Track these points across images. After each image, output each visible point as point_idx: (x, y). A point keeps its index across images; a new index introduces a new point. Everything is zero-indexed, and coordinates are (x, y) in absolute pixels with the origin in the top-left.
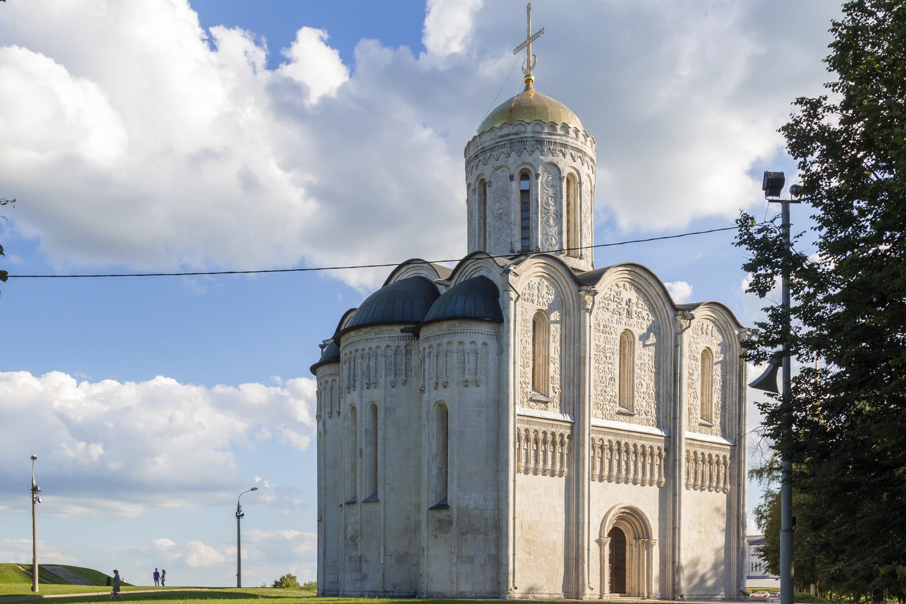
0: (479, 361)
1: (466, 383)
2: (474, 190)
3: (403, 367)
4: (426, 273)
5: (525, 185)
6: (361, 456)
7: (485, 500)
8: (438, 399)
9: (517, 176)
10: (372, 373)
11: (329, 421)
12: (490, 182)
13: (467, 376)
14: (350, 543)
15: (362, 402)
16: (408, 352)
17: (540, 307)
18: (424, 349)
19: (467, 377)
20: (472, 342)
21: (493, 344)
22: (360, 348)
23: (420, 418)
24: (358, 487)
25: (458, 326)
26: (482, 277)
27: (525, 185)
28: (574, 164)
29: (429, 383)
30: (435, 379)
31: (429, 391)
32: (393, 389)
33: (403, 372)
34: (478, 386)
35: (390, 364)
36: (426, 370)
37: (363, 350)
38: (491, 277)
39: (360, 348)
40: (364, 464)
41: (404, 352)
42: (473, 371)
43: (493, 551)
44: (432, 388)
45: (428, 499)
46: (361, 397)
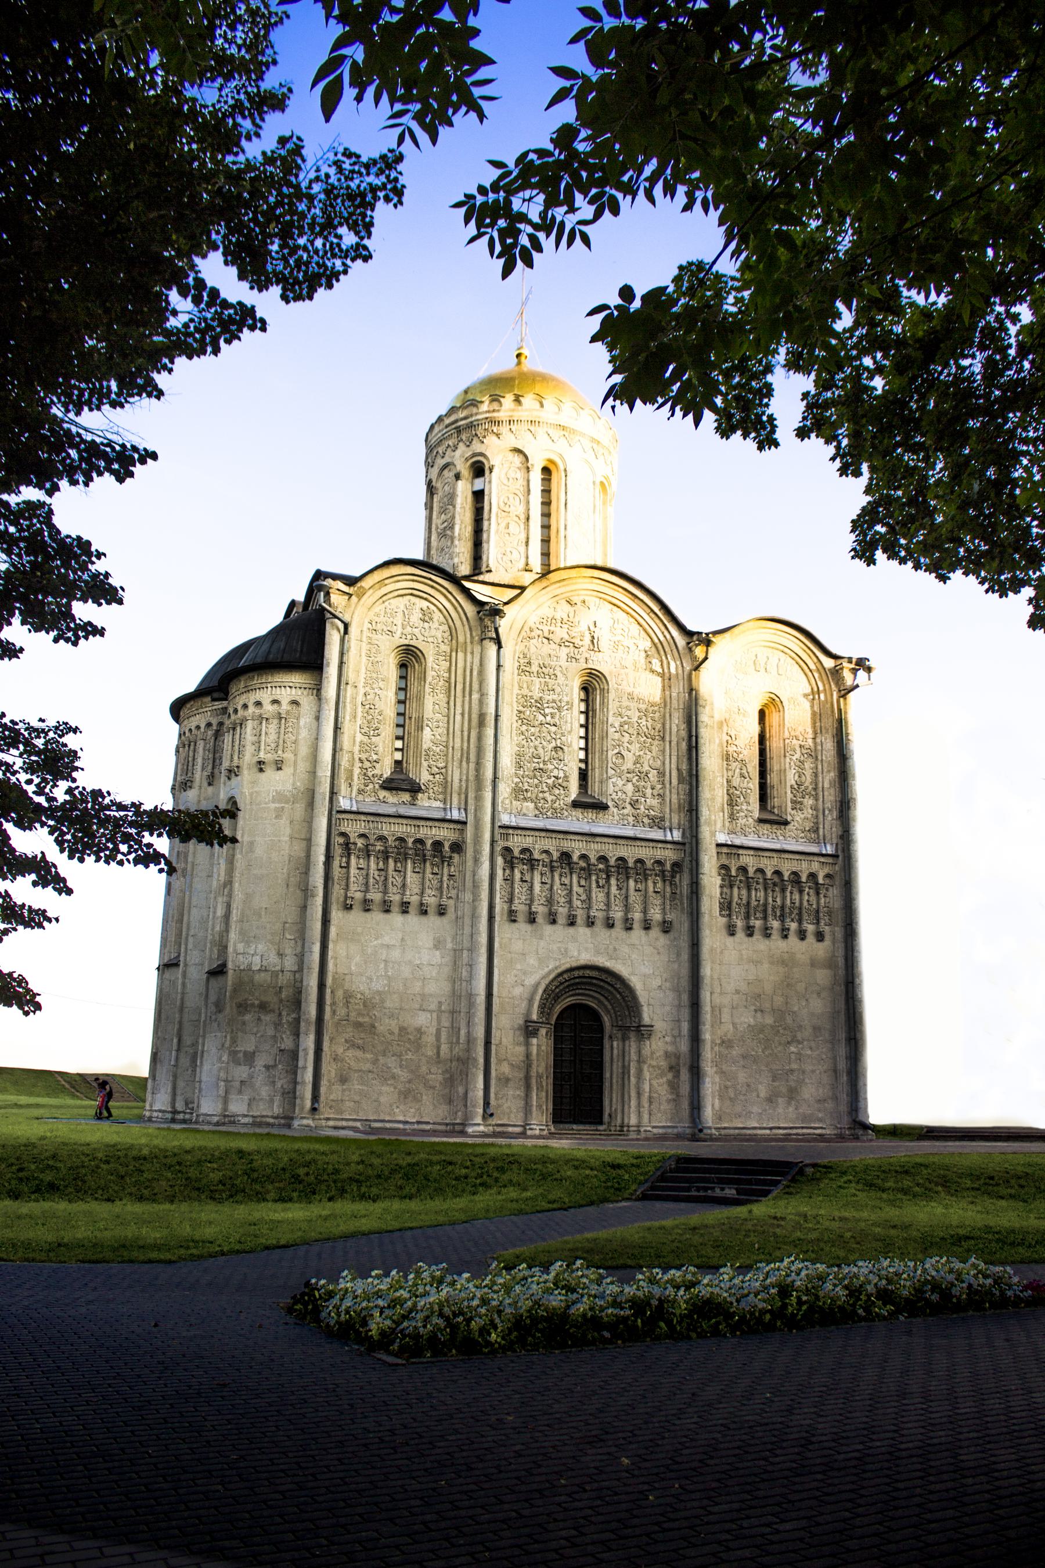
1: (261, 766)
5: (479, 484)
7: (281, 955)
9: (466, 473)
17: (406, 642)
20: (275, 702)
32: (210, 789)
42: (273, 745)
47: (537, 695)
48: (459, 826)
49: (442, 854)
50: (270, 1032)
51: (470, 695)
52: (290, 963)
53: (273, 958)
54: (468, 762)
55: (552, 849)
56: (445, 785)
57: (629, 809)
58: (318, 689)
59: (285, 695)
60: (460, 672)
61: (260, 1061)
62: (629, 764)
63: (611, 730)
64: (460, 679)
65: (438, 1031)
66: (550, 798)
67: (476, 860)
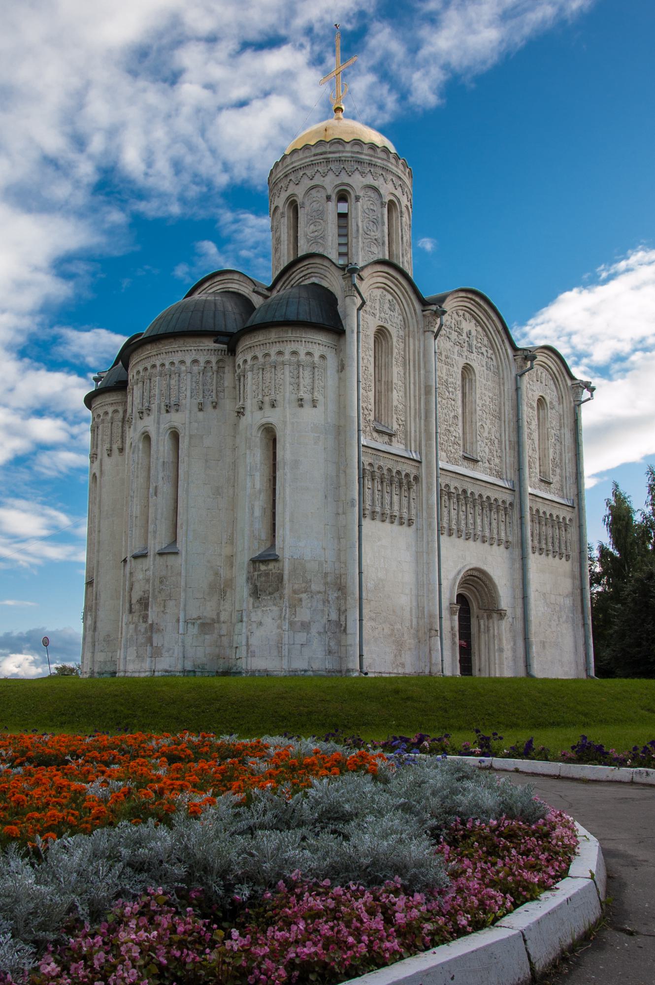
0: (316, 377)
1: (300, 402)
2: (283, 213)
3: (214, 387)
4: (236, 286)
5: (343, 208)
6: (156, 495)
8: (264, 421)
9: (334, 197)
10: (174, 393)
12: (303, 203)
13: (302, 393)
14: (136, 607)
15: (159, 428)
16: (220, 369)
17: (382, 324)
18: (245, 361)
19: (302, 394)
20: (309, 354)
21: (332, 362)
22: (158, 363)
23: (234, 448)
24: (150, 536)
25: (290, 334)
26: (314, 284)
27: (343, 208)
28: (396, 193)
29: (250, 404)
30: (260, 397)
31: (252, 412)
34: (315, 406)
35: (197, 383)
37: (163, 365)
38: (325, 284)
39: (158, 363)
40: (162, 503)
41: (215, 368)
42: (309, 388)
43: (334, 616)
45: (247, 548)
46: (158, 423)
47: (445, 378)
48: (417, 464)
49: (406, 483)
50: (320, 606)
51: (419, 371)
54: (420, 418)
55: (458, 486)
56: (406, 433)
57: (487, 465)
58: (339, 350)
59: (317, 351)
61: (314, 631)
62: (486, 434)
63: (478, 408)
64: (411, 358)
65: (411, 608)
66: (453, 451)
67: (429, 489)
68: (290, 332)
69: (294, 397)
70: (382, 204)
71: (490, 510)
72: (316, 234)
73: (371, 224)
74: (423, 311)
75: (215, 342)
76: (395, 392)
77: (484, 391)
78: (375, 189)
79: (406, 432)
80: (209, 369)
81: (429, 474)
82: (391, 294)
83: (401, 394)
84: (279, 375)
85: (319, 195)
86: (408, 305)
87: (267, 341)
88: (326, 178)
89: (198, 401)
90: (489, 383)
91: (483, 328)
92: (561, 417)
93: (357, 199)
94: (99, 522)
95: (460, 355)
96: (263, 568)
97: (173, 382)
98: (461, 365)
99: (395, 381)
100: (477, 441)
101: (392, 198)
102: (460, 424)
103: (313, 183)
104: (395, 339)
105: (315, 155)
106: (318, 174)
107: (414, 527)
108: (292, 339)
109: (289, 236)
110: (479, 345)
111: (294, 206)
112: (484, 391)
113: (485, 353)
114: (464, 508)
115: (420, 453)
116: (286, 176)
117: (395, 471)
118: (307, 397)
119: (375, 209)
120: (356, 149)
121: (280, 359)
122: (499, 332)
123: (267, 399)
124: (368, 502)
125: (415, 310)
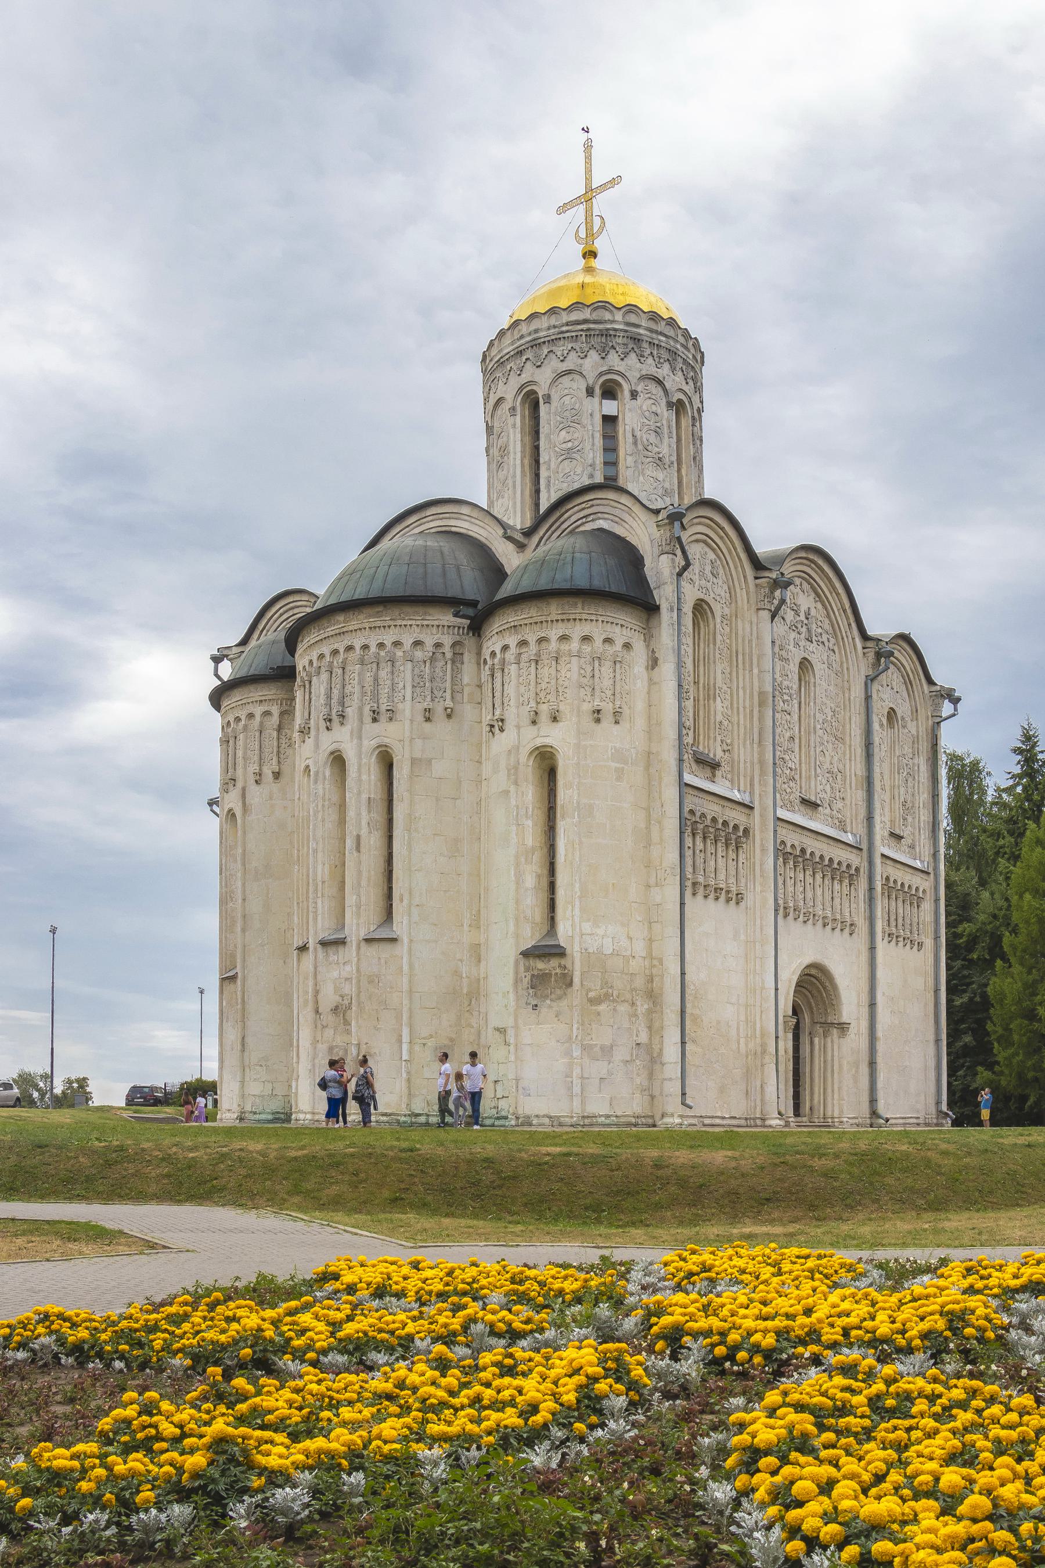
0: (618, 677)
2: (513, 409)
3: (448, 685)
5: (610, 407)
8: (539, 742)
9: (598, 391)
11: (253, 788)
12: (549, 396)
17: (702, 596)
25: (579, 609)
27: (610, 407)
28: (686, 388)
30: (533, 704)
31: (518, 727)
33: (448, 695)
34: (617, 722)
36: (511, 690)
42: (609, 693)
44: (526, 721)
48: (747, 811)
51: (751, 670)
52: (639, 948)
53: (624, 943)
58: (648, 636)
59: (620, 636)
60: (740, 640)
68: (580, 605)
69: (587, 707)
70: (670, 405)
71: (833, 879)
72: (570, 445)
73: (653, 434)
74: (756, 578)
75: (456, 615)
76: (718, 699)
77: (824, 700)
78: (660, 382)
79: (733, 761)
80: (439, 656)
81: (763, 823)
82: (713, 550)
83: (727, 703)
84: (563, 672)
85: (575, 386)
86: (736, 568)
87: (543, 618)
88: (588, 361)
89: (425, 705)
90: (831, 688)
91: (824, 605)
92: (916, 740)
93: (634, 395)
94: (244, 885)
95: (797, 645)
96: (540, 965)
97: (383, 674)
98: (797, 660)
99: (719, 683)
100: (816, 776)
101: (682, 397)
102: (797, 750)
103: (564, 367)
104: (718, 620)
105: (567, 324)
106: (573, 354)
107: (743, 904)
108: (584, 616)
109: (523, 446)
110: (820, 630)
111: (532, 402)
112: (824, 700)
113: (826, 643)
114: (801, 875)
115: (752, 793)
116: (520, 353)
117: (721, 821)
118: (607, 707)
119: (659, 412)
120: (632, 318)
121: (565, 647)
122: (845, 611)
123: (544, 708)
124: (689, 869)
125: (745, 577)
